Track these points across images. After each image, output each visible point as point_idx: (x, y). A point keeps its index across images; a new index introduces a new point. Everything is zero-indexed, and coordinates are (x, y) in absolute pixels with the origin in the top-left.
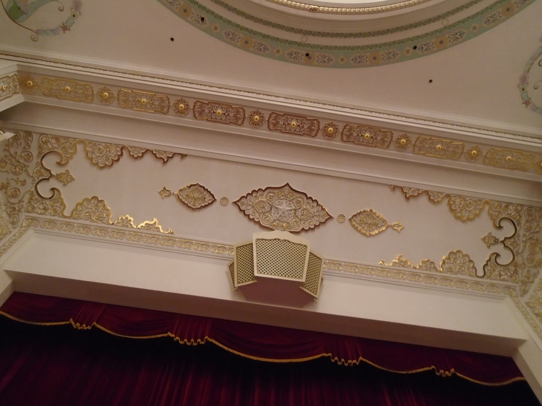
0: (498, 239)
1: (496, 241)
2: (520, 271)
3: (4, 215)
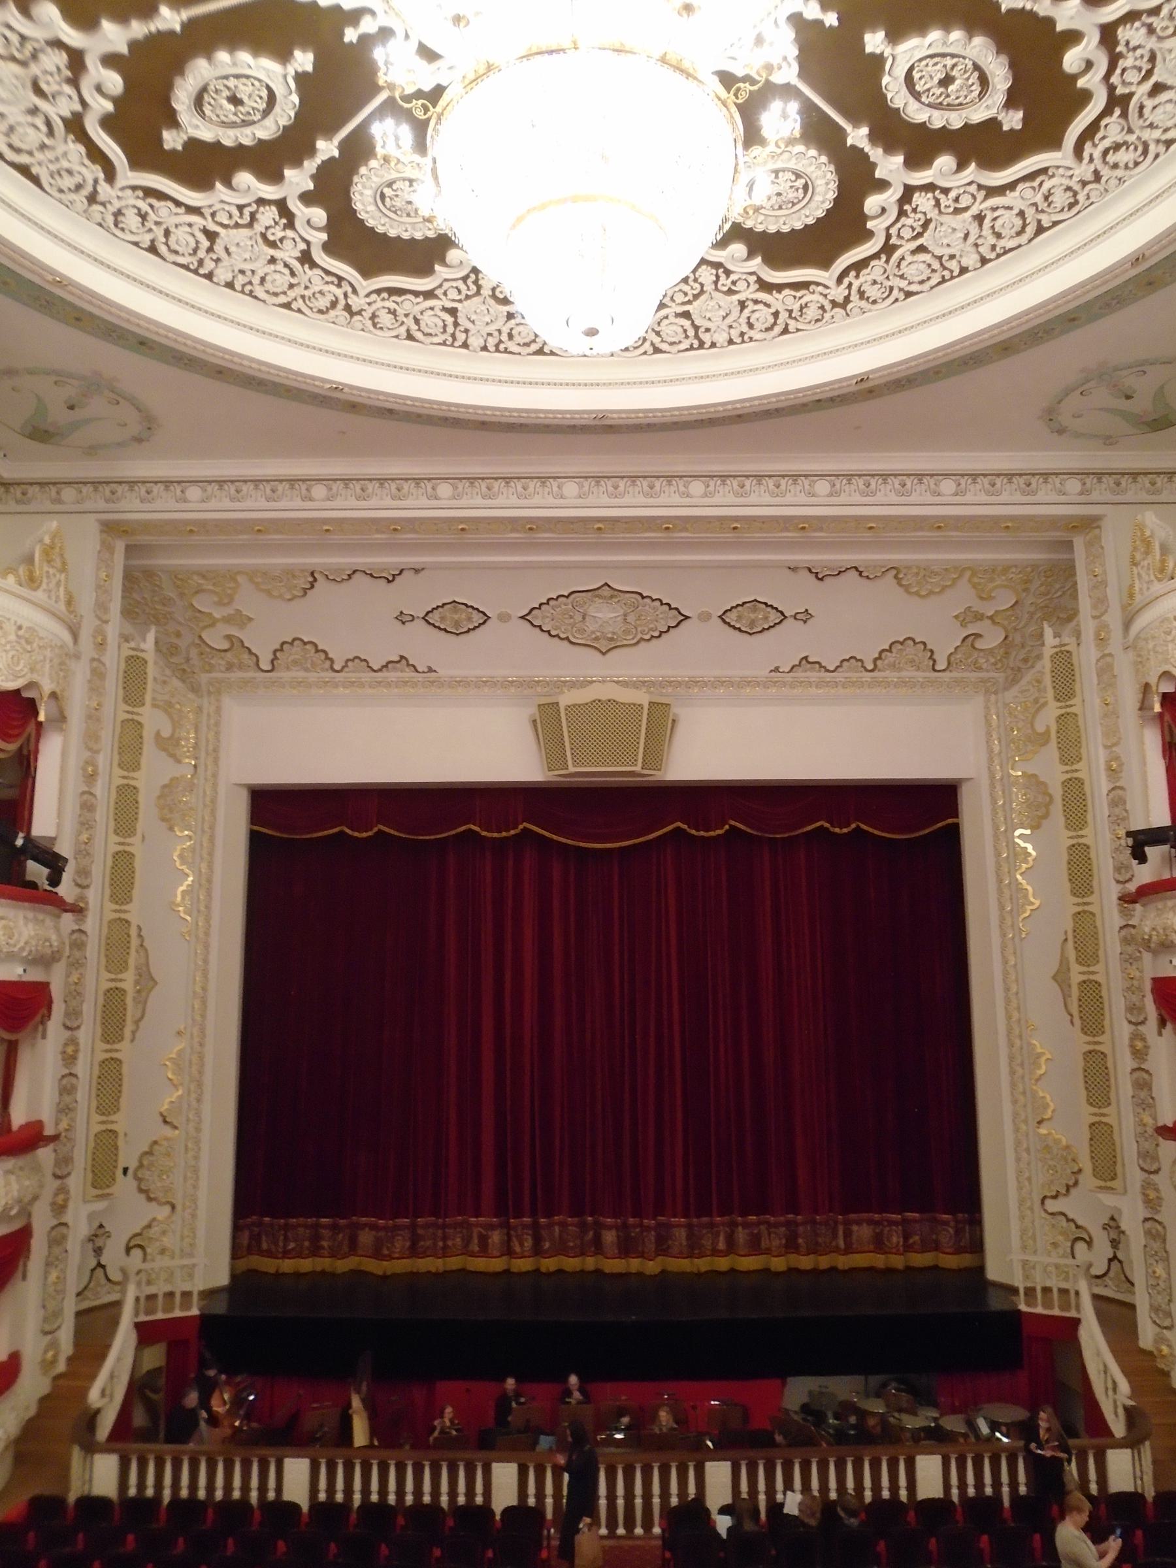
0: (982, 615)
1: (979, 617)
2: (1014, 653)
3: (176, 683)
